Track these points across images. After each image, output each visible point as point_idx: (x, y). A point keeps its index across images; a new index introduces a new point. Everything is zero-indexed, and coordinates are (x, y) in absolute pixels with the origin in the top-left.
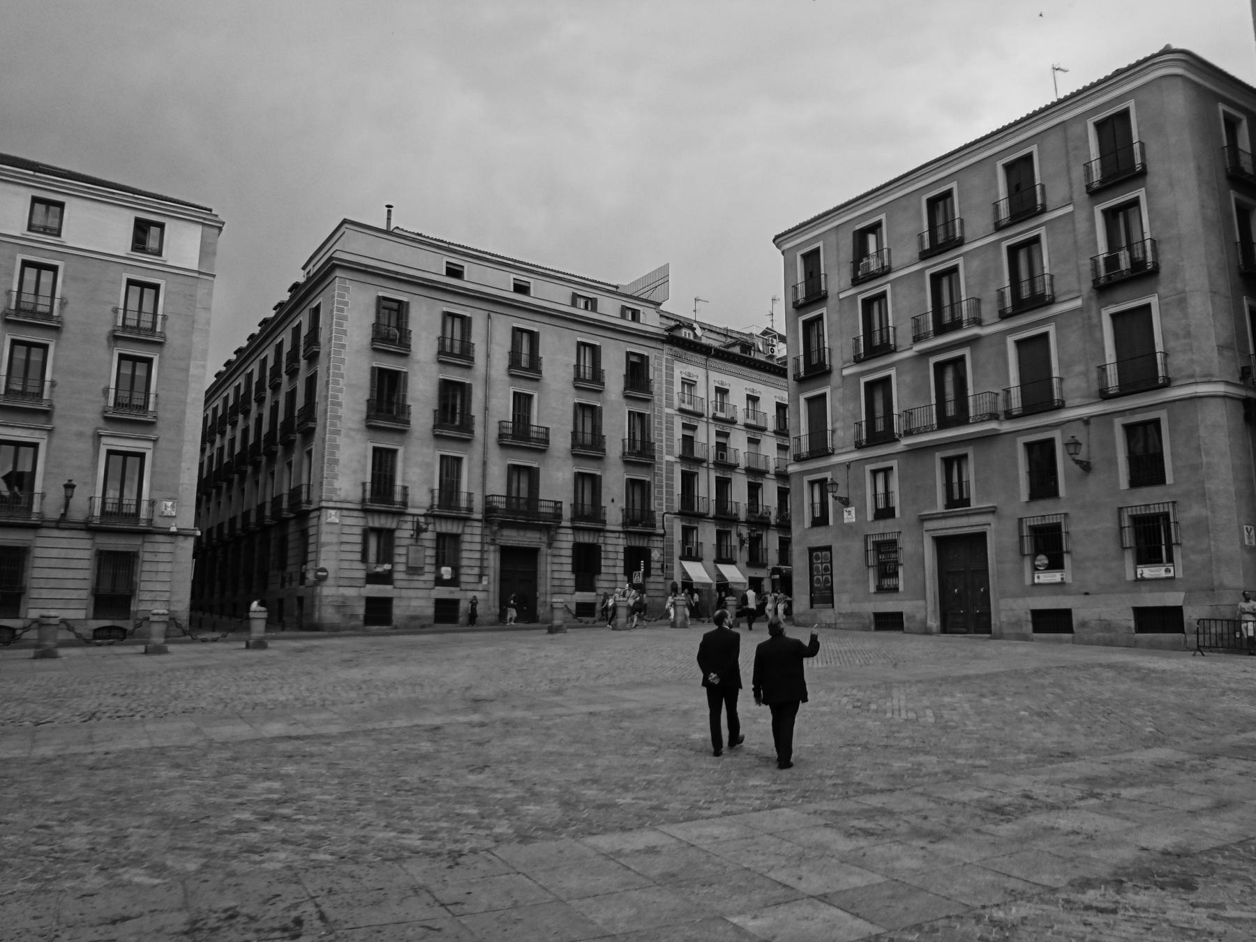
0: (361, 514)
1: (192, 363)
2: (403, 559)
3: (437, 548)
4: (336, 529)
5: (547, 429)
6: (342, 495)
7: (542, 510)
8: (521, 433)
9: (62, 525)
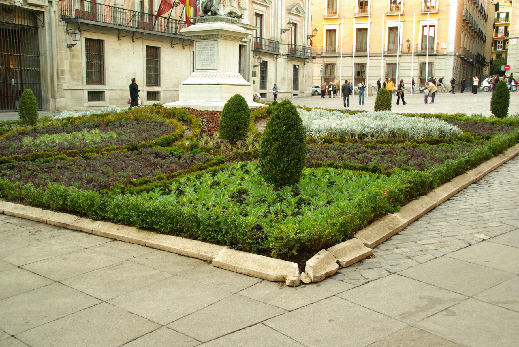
9: (408, 54)
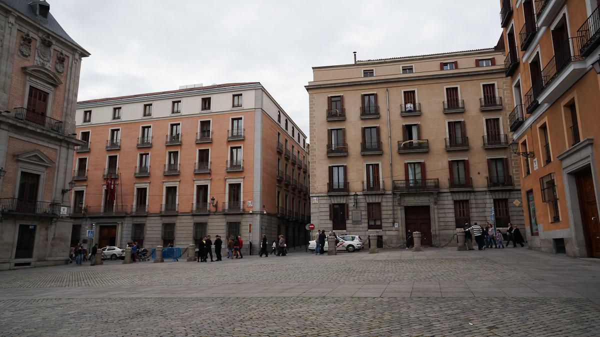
0: (328, 198)
1: (255, 145)
3: (495, 207)
4: (317, 206)
5: (428, 140)
6: (319, 190)
7: (429, 184)
8: (412, 145)
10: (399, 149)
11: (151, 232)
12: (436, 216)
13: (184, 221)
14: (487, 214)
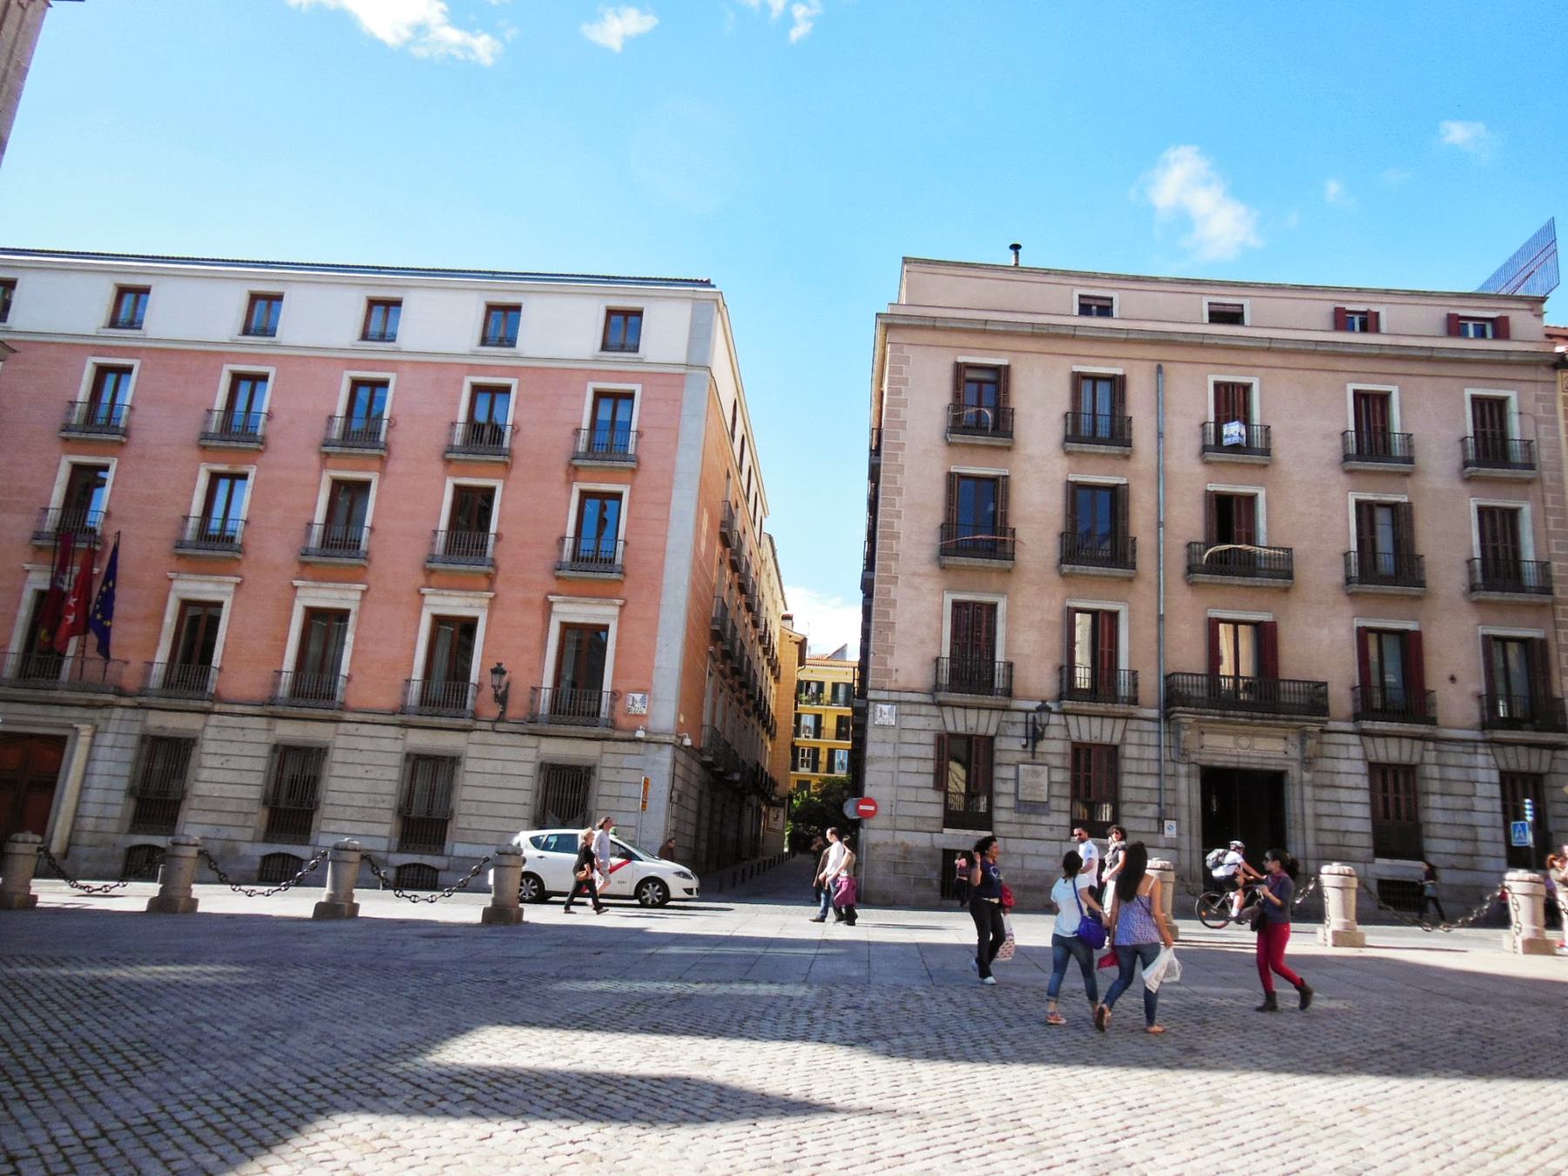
0: (934, 710)
2: (1009, 787)
5: (1289, 550)
6: (902, 680)
9: (499, 726)
10: (1191, 569)
11: (220, 776)
12: (1309, 810)
13: (364, 744)
14: (1478, 818)
